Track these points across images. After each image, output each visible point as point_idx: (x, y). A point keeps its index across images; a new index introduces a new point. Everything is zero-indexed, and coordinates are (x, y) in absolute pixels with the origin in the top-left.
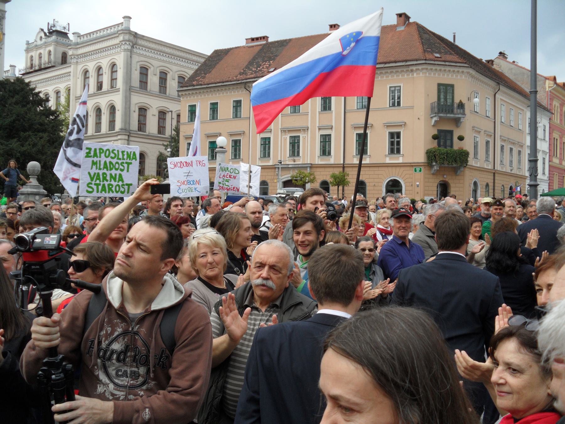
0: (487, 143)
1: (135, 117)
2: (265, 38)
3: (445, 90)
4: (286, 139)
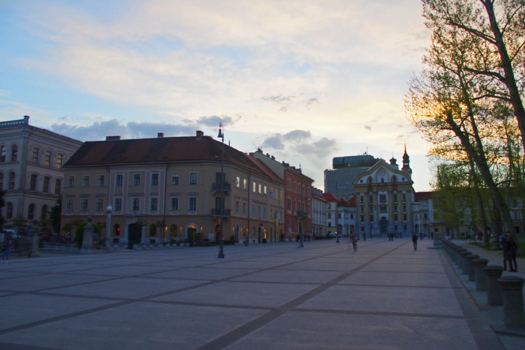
0: (244, 204)
1: (29, 180)
2: (118, 137)
3: (220, 176)
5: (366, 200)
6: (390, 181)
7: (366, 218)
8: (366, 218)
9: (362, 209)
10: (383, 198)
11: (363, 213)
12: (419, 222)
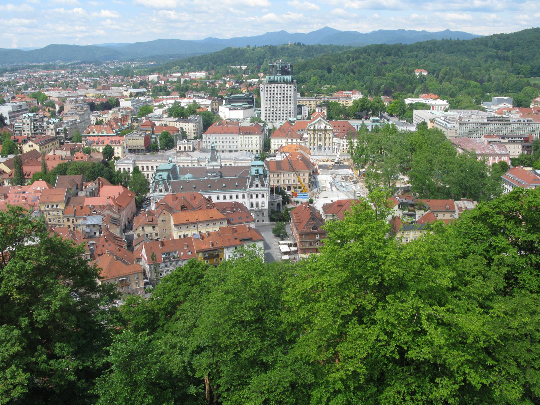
7: (312, 144)
8: (312, 144)
12: (336, 147)
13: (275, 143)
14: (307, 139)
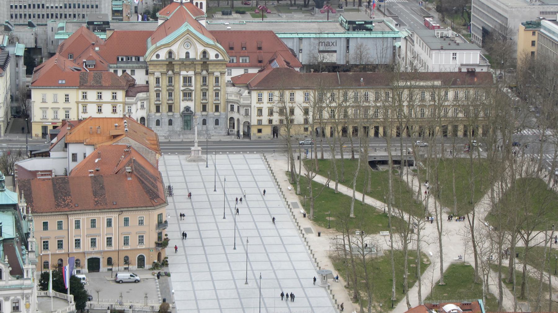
4: (88, 240)
5: (164, 82)
6: (198, 58)
8: (164, 108)
9: (158, 95)
10: (187, 80)
11: (160, 101)
12: (235, 116)
13: (47, 106)
14: (146, 88)
